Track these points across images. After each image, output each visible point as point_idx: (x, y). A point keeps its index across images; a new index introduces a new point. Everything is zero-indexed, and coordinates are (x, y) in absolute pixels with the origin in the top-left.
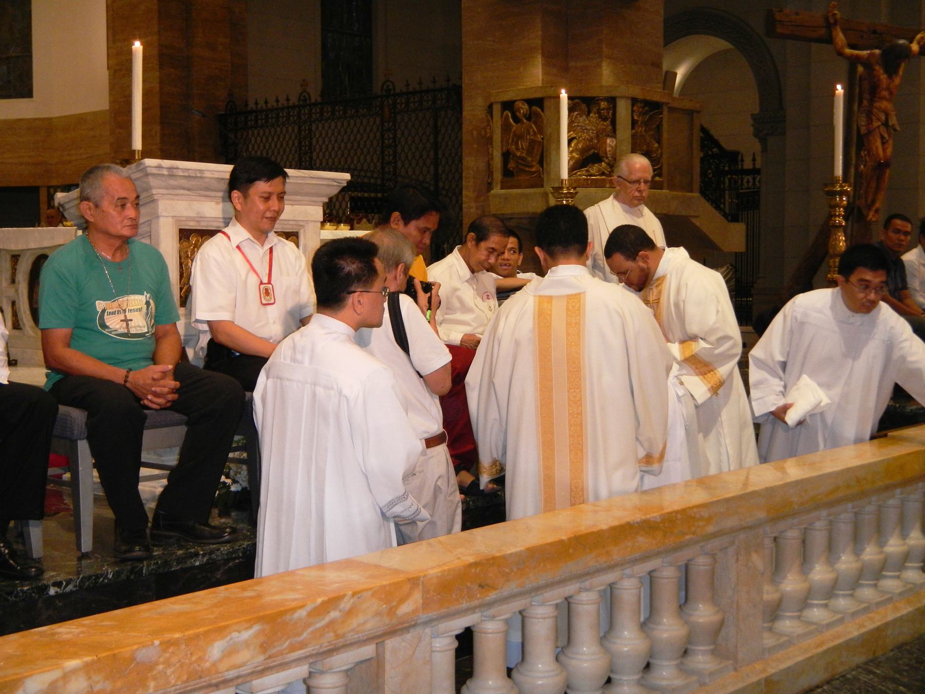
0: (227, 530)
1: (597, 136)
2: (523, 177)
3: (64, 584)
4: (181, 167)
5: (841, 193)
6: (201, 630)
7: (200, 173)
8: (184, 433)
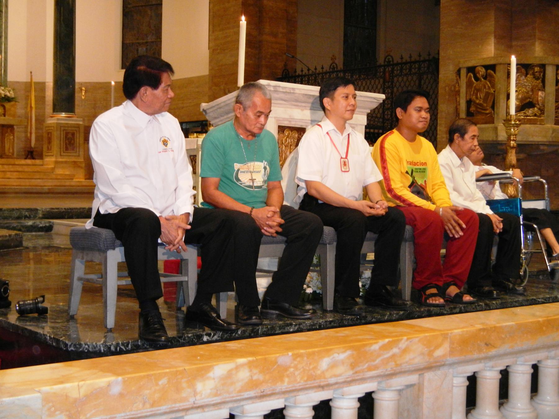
0: (310, 311)
1: (532, 90)
2: (479, 117)
3: (212, 334)
4: (281, 86)
6: (316, 349)
7: (293, 90)
8: (283, 248)
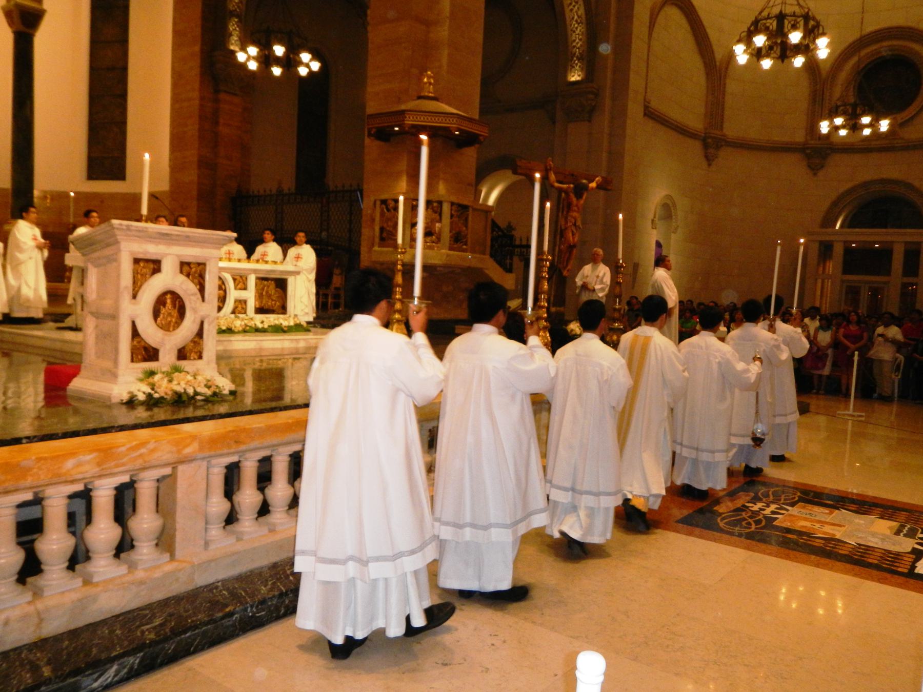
2: (391, 242)
5: (547, 260)
